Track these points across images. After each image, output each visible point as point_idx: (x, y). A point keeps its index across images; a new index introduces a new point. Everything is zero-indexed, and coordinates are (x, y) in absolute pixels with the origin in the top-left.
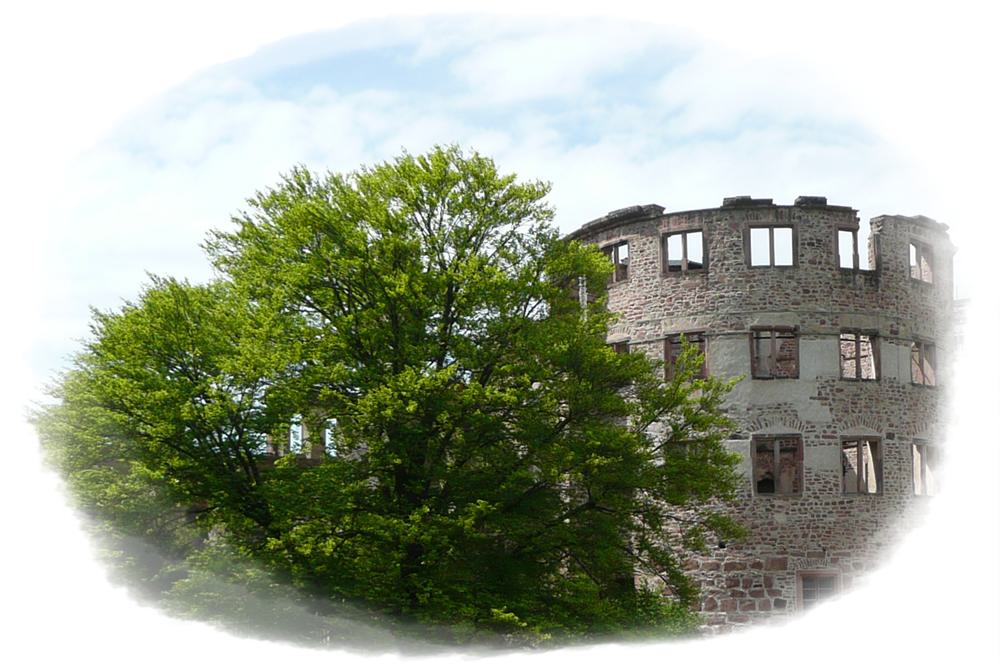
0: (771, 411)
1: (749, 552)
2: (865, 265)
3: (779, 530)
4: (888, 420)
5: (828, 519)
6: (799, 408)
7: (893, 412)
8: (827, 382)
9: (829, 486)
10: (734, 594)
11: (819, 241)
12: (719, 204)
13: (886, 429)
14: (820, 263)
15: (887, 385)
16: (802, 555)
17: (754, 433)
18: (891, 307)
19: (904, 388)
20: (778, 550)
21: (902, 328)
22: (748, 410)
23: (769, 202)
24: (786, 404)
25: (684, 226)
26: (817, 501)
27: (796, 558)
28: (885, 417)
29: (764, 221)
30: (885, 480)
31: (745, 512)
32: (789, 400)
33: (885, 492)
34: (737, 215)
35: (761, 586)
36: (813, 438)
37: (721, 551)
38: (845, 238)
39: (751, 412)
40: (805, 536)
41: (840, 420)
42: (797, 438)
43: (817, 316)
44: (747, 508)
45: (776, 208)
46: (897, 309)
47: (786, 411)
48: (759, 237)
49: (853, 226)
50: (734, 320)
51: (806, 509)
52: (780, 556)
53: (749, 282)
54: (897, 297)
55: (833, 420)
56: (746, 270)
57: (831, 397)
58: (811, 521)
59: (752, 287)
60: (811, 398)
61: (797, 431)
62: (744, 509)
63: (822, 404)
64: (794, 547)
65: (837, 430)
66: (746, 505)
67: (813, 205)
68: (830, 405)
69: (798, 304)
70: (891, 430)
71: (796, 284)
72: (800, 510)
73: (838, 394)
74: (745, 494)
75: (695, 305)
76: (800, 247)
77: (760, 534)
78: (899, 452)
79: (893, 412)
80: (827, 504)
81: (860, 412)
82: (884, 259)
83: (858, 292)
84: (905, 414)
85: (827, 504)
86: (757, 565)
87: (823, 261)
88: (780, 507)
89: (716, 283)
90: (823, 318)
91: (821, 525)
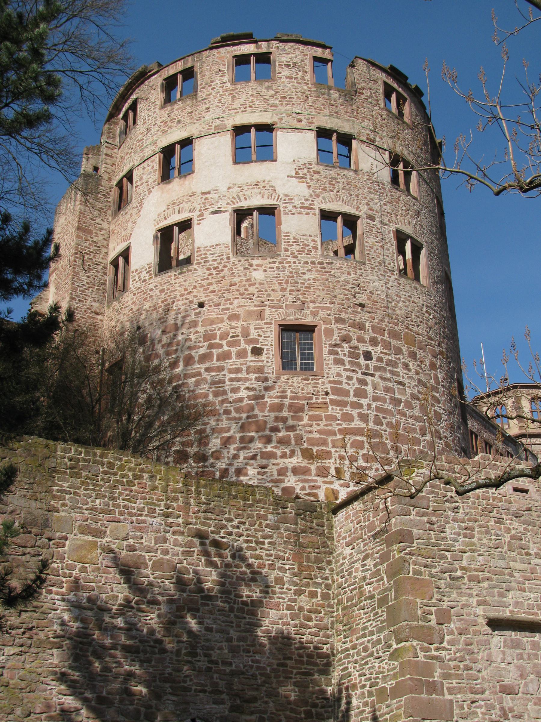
0: (250, 187)
3: (257, 286)
5: (304, 277)
6: (278, 185)
8: (305, 164)
9: (307, 248)
10: (211, 346)
11: (295, 64)
14: (296, 78)
15: (366, 178)
16: (281, 307)
20: (256, 303)
22: (229, 188)
24: (264, 181)
26: (295, 260)
32: (267, 179)
35: (238, 336)
39: (231, 190)
43: (294, 115)
44: (226, 269)
47: (264, 187)
50: (218, 122)
51: (285, 267)
52: (258, 308)
55: (311, 195)
58: (288, 277)
60: (288, 176)
61: (275, 202)
62: (223, 270)
63: (300, 182)
64: (273, 300)
65: (315, 203)
66: (225, 266)
68: (307, 182)
69: (276, 106)
71: (273, 93)
72: (278, 268)
73: (315, 175)
74: (224, 257)
77: (237, 290)
80: (307, 263)
81: (338, 192)
83: (332, 102)
85: (307, 263)
86: (234, 317)
88: (257, 265)
89: (204, 99)
90: (299, 117)
91: (299, 281)
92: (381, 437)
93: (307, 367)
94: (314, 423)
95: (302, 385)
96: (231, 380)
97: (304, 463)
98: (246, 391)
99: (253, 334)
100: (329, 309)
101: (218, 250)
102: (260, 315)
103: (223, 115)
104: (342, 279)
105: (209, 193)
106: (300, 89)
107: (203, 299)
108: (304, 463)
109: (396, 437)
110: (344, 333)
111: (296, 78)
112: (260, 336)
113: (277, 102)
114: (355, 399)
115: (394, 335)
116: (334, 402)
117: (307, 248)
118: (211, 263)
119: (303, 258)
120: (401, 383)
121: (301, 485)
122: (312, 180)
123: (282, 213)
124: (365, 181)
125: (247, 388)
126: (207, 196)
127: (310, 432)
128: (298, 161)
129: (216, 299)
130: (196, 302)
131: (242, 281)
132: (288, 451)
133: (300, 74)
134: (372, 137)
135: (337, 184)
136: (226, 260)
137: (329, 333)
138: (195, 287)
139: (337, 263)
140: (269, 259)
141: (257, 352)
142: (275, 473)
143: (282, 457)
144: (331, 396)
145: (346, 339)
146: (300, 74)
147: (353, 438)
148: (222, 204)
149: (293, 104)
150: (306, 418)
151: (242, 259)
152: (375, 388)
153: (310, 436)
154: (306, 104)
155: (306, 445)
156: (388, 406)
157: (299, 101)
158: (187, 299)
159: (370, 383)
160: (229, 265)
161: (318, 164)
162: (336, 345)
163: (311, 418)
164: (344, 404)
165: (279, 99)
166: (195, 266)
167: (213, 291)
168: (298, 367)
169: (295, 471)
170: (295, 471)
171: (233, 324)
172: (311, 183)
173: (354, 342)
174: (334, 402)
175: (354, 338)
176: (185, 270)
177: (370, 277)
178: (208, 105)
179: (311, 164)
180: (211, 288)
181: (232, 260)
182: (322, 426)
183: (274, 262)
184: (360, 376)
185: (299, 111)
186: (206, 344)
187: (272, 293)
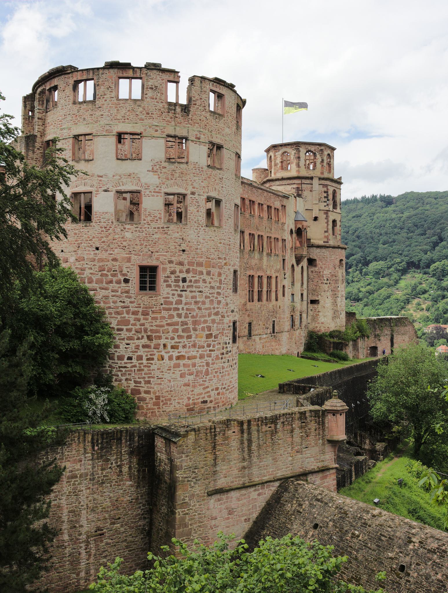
0: (126, 177)
1: (111, 252)
2: (183, 101)
3: (128, 242)
4: (192, 184)
7: (195, 181)
9: (156, 218)
11: (156, 87)
12: (102, 65)
13: (190, 189)
15: (192, 166)
17: (116, 189)
18: (197, 125)
19: (202, 168)
21: (202, 136)
23: (129, 64)
25: (85, 77)
26: (149, 226)
27: (136, 257)
28: (191, 183)
29: (125, 75)
30: (188, 217)
31: (109, 231)
32: (136, 172)
33: (188, 223)
34: (111, 71)
35: (116, 271)
36: (148, 193)
37: (97, 251)
38: (171, 86)
40: (142, 245)
41: (164, 184)
42: (138, 192)
43: (153, 127)
44: (111, 229)
45: (133, 68)
46: (200, 126)
47: (134, 178)
48: (124, 84)
49: (176, 80)
50: (108, 127)
51: (143, 231)
52: (128, 255)
53: (117, 107)
54: (200, 120)
55: (160, 183)
56: (115, 101)
57: (159, 171)
59: (118, 110)
65: (162, 188)
66: (110, 227)
67: (153, 67)
68: (158, 175)
70: (193, 190)
72: (139, 231)
73: (163, 170)
74: (110, 221)
75: (89, 119)
76: (145, 90)
78: (198, 202)
79: (195, 181)
80: (155, 228)
81: (176, 179)
82: (193, 99)
84: (202, 182)
85: (155, 228)
86: (115, 260)
87: (158, 98)
88: (128, 229)
89: (100, 107)
90: (157, 128)
92: (187, 324)
93: (152, 288)
94: (154, 321)
95: (149, 301)
96: (113, 296)
97: (148, 343)
98: (120, 303)
99: (125, 271)
100: (165, 256)
101: (107, 216)
102: (129, 260)
103: (111, 123)
104: (174, 236)
105: (102, 177)
106: (158, 107)
107: (98, 246)
108: (148, 343)
109: (195, 323)
110: (172, 269)
111: (156, 99)
112: (128, 272)
113: (143, 117)
114: (176, 306)
115: (200, 264)
116: (164, 309)
117: (156, 218)
118: (103, 224)
119: (153, 225)
120: (200, 292)
121: (146, 354)
122: (161, 173)
123: (143, 195)
124: (192, 169)
125: (121, 301)
126: (101, 178)
127: (152, 326)
128: (154, 160)
129: (105, 247)
130: (94, 246)
131: (119, 238)
132: (140, 336)
133: (159, 95)
134: (198, 136)
135: (175, 174)
136: (111, 223)
137: (165, 269)
138: (94, 238)
139: (172, 227)
140: (134, 225)
141: (126, 281)
142: (134, 348)
143: (137, 339)
144: (164, 306)
145: (173, 272)
146: (159, 95)
147: (173, 327)
148: (109, 186)
149: (153, 118)
150: (150, 318)
151: (120, 224)
152: (186, 298)
153: (152, 328)
154: (161, 118)
155: (149, 334)
156: (193, 306)
157: (157, 116)
158: (89, 243)
159: (184, 295)
160: (113, 227)
161: (165, 161)
162: (168, 277)
163: (153, 318)
164: (170, 309)
165: (145, 115)
166: (92, 224)
167: (104, 242)
168: (148, 288)
169: (144, 346)
170: (144, 346)
171: (114, 263)
172: (161, 175)
173: (178, 273)
174: (164, 309)
175: (178, 271)
176: (88, 225)
177: (189, 232)
178: (102, 113)
179: (161, 162)
180: (103, 240)
181: (114, 224)
182: (158, 323)
183: (137, 227)
184: (179, 292)
185: (157, 124)
186: (100, 273)
187: (135, 246)
